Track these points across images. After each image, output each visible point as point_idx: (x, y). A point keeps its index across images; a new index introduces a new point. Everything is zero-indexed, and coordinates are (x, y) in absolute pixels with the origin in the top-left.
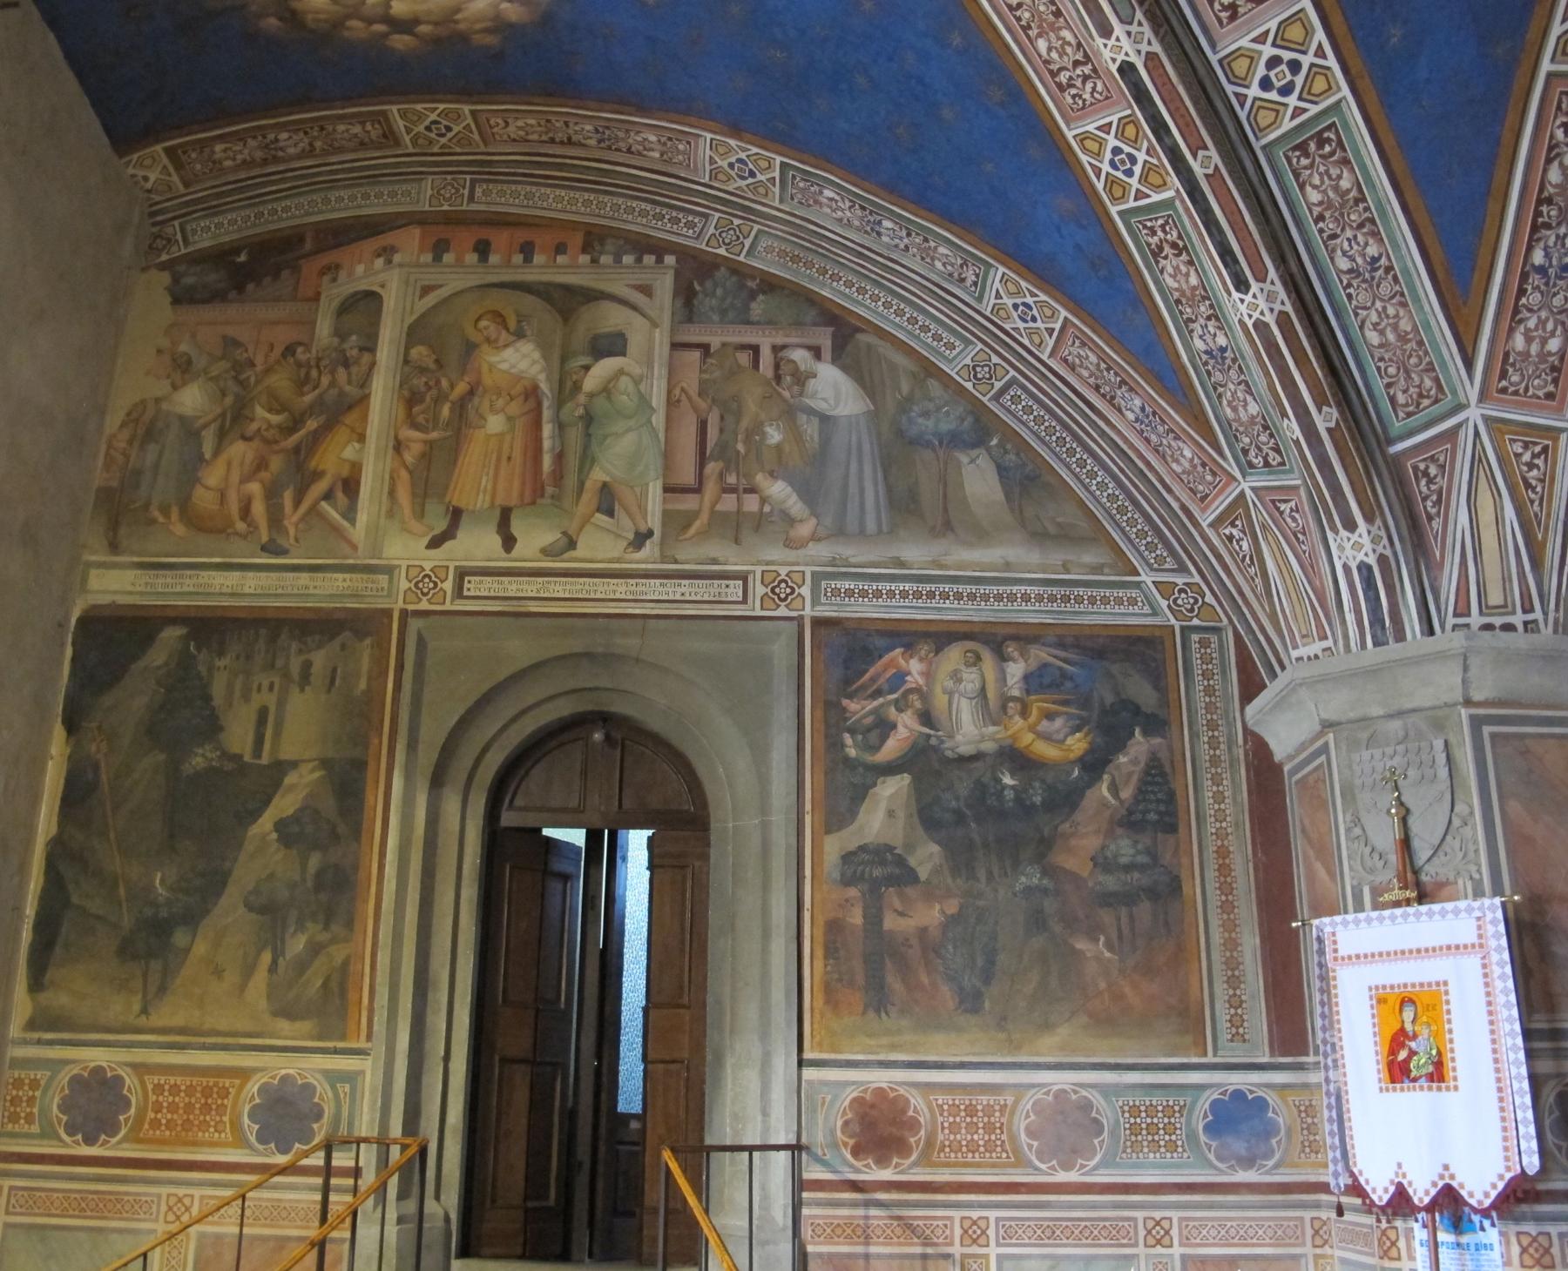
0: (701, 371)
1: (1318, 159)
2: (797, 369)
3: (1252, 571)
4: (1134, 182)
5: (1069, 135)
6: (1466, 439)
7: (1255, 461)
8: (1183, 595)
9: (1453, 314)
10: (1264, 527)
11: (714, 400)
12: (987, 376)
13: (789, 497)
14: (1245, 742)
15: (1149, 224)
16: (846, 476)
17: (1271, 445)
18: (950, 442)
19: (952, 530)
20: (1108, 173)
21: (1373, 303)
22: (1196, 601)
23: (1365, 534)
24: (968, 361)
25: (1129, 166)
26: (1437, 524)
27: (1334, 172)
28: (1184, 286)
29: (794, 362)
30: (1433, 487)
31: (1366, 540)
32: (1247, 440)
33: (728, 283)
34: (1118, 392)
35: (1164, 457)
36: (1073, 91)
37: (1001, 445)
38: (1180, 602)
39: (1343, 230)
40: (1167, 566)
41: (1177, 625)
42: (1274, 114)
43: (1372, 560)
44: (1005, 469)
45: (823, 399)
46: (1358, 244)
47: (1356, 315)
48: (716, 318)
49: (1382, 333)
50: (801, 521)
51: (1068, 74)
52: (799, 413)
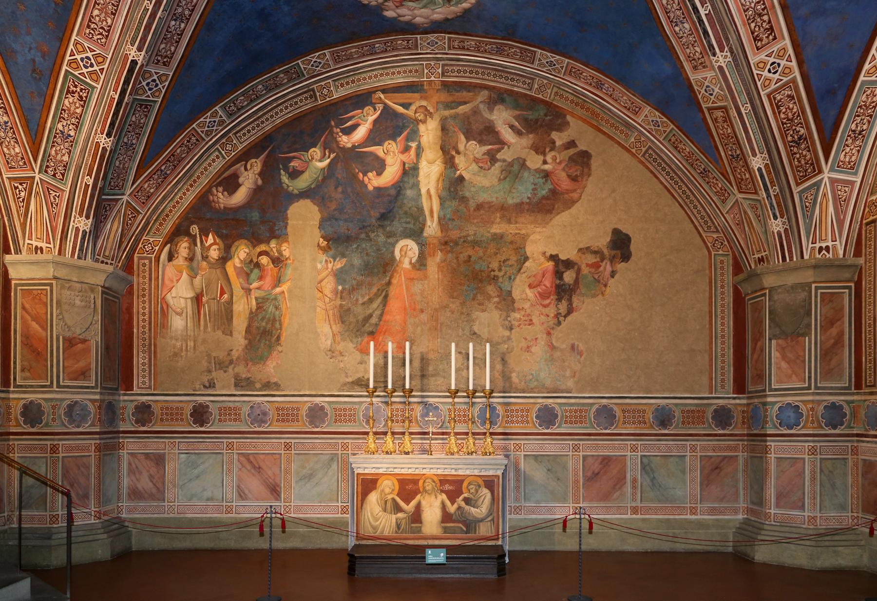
6: (120, 203)
10: (37, 193)
26: (102, 224)
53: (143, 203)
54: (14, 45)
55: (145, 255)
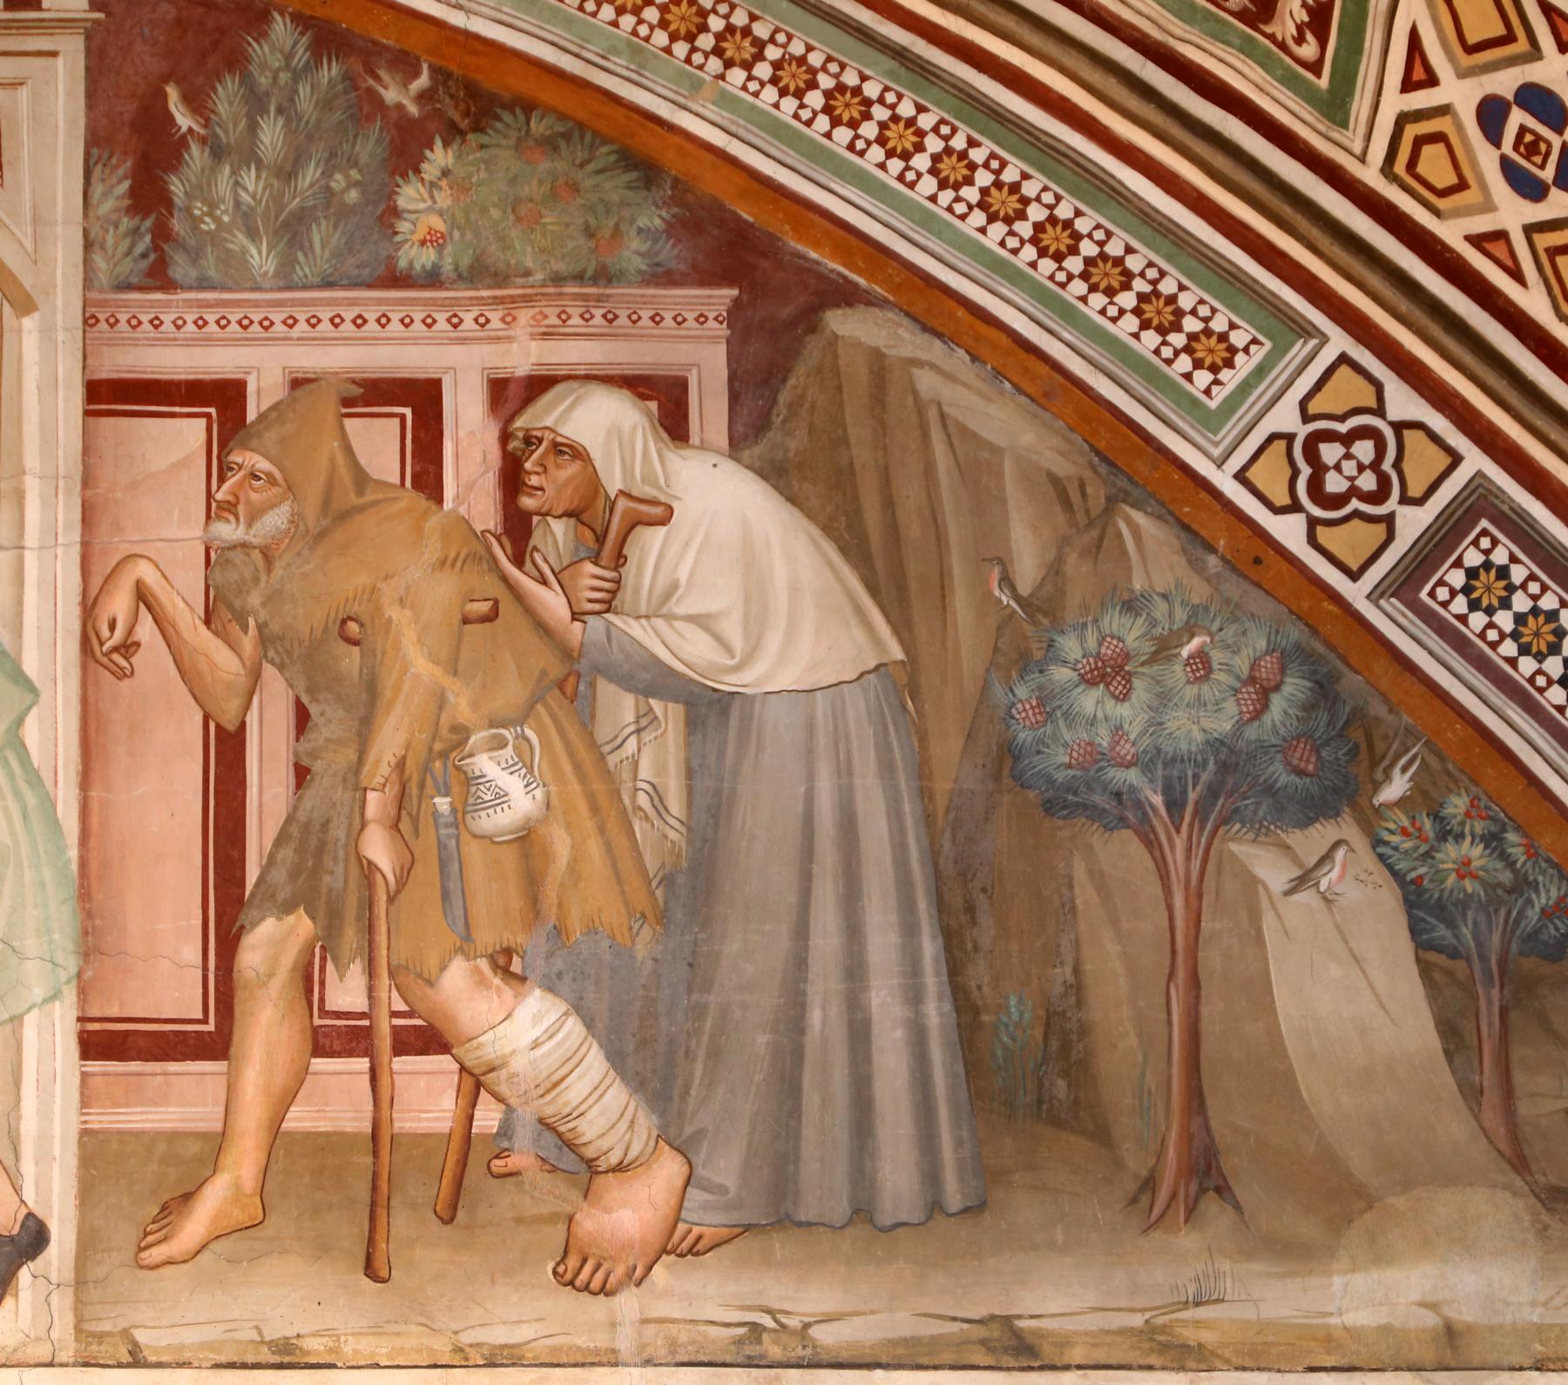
0: (214, 510)
2: (593, 484)
11: (265, 639)
12: (1368, 482)
13: (573, 1061)
16: (800, 963)
18: (1213, 793)
19: (1223, 1190)
24: (1285, 417)
29: (577, 453)
33: (304, 90)
37: (1423, 798)
44: (1440, 910)
45: (702, 621)
48: (261, 258)
50: (619, 1168)
52: (606, 690)
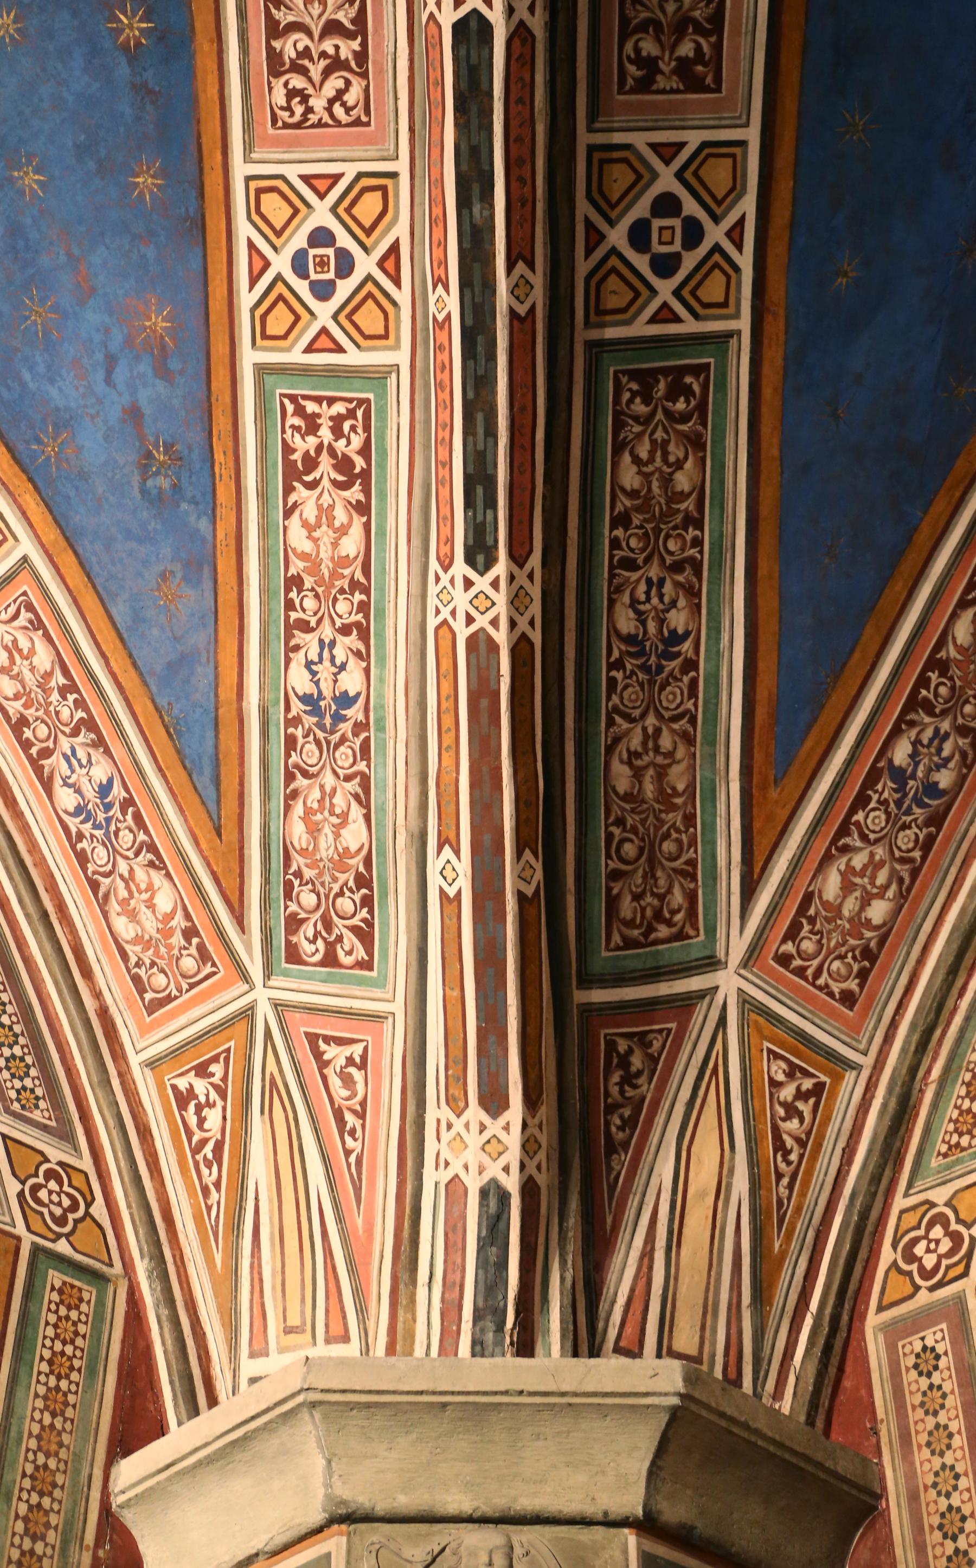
1: (660, 415)
3: (209, 1177)
4: (324, 311)
5: (240, 170)
7: (308, 948)
8: (53, 1185)
9: (755, 791)
14: (99, 1543)
15: (311, 407)
17: (356, 921)
20: (279, 278)
21: (643, 716)
22: (74, 1207)
23: (516, 1128)
25: (331, 275)
27: (676, 452)
28: (325, 553)
30: (630, 1092)
31: (513, 1140)
32: (309, 899)
34: (65, 744)
35: (103, 904)
36: (297, 82)
38: (43, 1194)
39: (647, 560)
40: (36, 1115)
41: (28, 1239)
42: (630, 295)
43: (512, 1184)
46: (661, 597)
47: (611, 723)
49: (638, 774)
51: (303, 41)
53: (848, 999)
54: (53, 392)
55: (923, 1297)
